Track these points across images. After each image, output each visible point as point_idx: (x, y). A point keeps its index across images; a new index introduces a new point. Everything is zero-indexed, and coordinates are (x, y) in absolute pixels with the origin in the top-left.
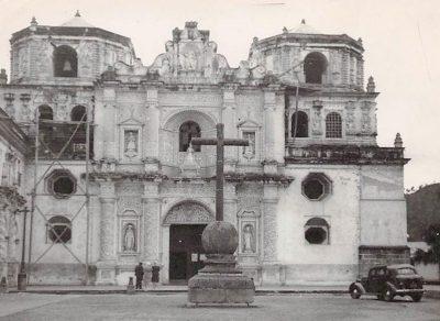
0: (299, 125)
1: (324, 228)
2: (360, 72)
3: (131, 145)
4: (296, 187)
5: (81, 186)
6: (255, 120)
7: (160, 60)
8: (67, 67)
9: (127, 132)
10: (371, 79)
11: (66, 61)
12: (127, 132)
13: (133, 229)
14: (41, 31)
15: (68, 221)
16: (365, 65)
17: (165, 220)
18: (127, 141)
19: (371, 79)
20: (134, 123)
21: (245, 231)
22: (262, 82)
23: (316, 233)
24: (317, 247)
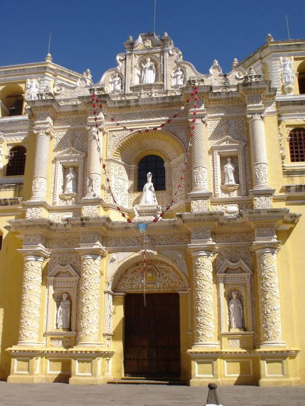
17: (115, 289)
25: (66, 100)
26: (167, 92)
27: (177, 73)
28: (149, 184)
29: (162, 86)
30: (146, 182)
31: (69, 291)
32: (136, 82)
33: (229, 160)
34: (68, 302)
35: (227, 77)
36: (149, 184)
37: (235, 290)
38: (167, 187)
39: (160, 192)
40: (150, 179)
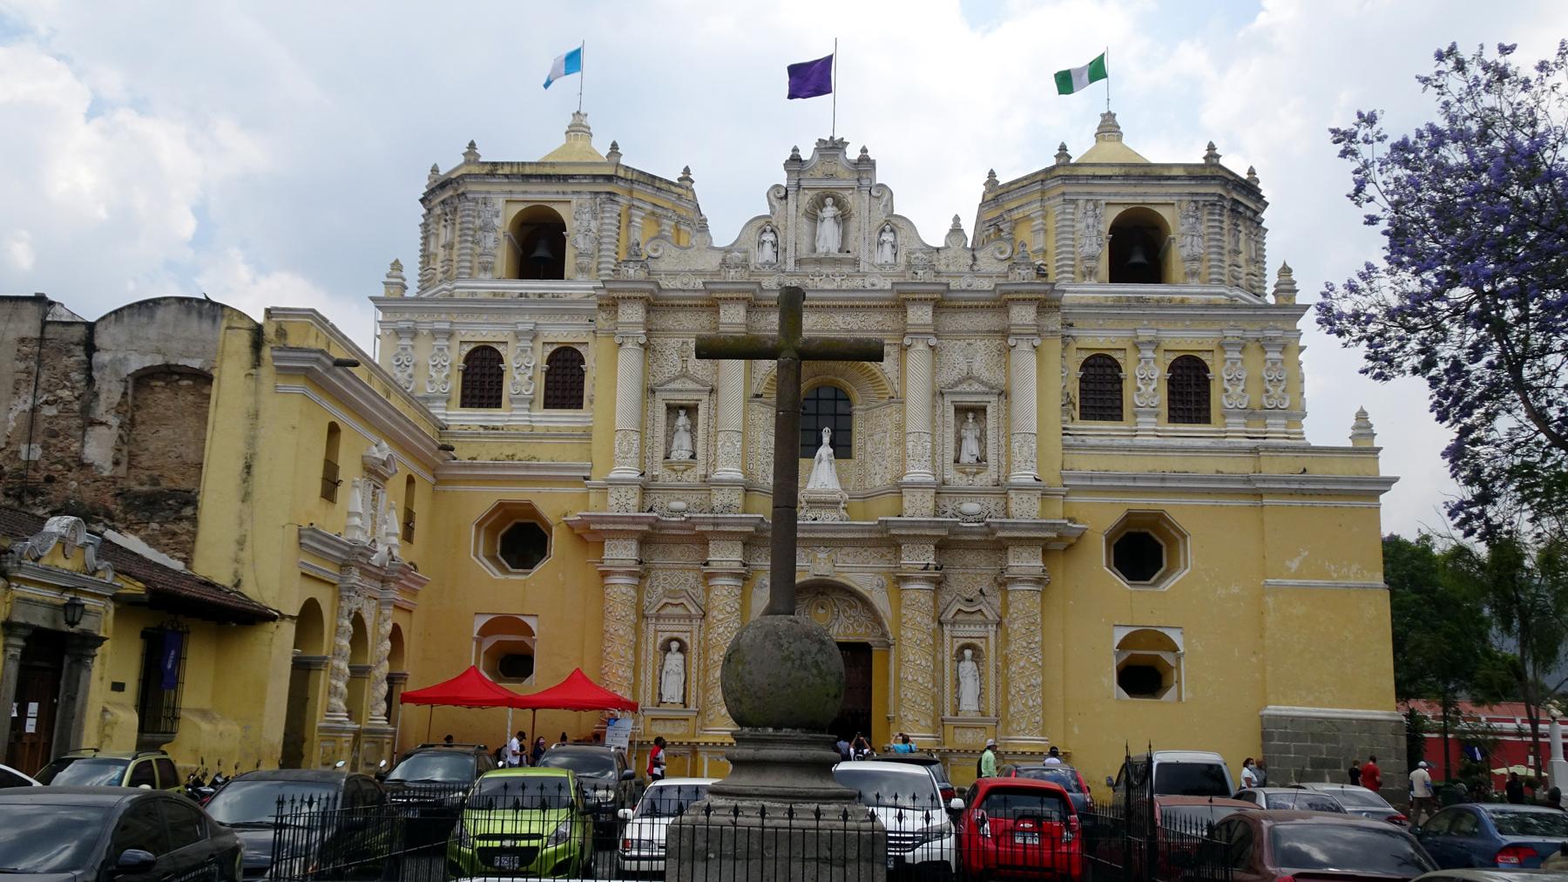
0: (1100, 389)
1: (1168, 658)
2: (1258, 260)
3: (682, 442)
4: (1098, 553)
5: (558, 542)
6: (985, 375)
7: (753, 234)
8: (541, 252)
9: (673, 410)
10: (1286, 271)
11: (539, 247)
12: (673, 410)
13: (682, 649)
14: (493, 171)
15: (529, 632)
16: (1269, 240)
18: (671, 432)
19: (1286, 271)
20: (690, 385)
21: (959, 656)
22: (1001, 281)
23: (1143, 676)
24: (1144, 705)
25: (673, 274)
26: (864, 275)
27: (885, 237)
28: (825, 451)
29: (856, 262)
30: (819, 443)
31: (682, 636)
32: (804, 251)
33: (971, 415)
34: (680, 656)
35: (978, 255)
36: (825, 451)
37: (968, 646)
38: (855, 451)
39: (843, 462)
40: (826, 439)
